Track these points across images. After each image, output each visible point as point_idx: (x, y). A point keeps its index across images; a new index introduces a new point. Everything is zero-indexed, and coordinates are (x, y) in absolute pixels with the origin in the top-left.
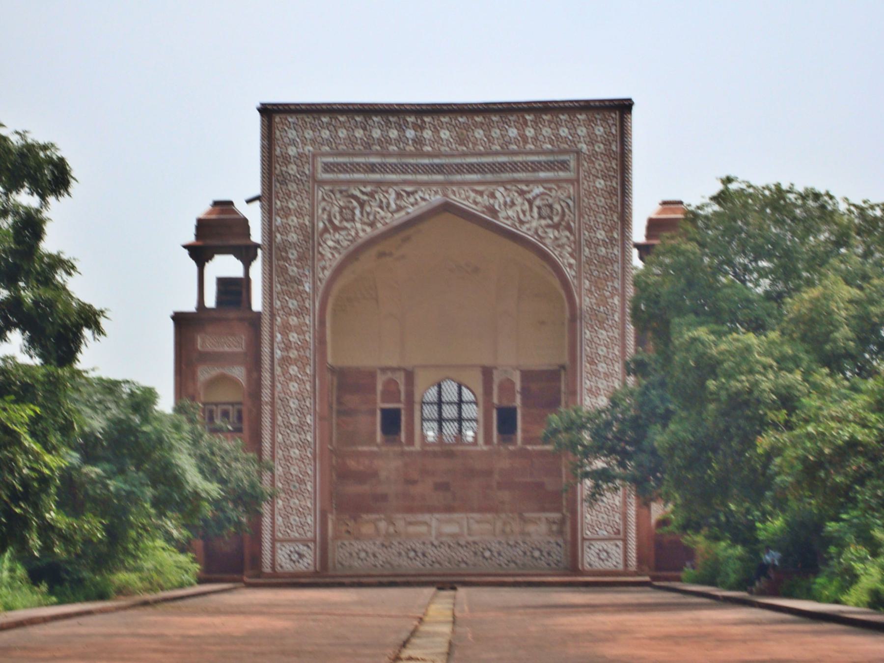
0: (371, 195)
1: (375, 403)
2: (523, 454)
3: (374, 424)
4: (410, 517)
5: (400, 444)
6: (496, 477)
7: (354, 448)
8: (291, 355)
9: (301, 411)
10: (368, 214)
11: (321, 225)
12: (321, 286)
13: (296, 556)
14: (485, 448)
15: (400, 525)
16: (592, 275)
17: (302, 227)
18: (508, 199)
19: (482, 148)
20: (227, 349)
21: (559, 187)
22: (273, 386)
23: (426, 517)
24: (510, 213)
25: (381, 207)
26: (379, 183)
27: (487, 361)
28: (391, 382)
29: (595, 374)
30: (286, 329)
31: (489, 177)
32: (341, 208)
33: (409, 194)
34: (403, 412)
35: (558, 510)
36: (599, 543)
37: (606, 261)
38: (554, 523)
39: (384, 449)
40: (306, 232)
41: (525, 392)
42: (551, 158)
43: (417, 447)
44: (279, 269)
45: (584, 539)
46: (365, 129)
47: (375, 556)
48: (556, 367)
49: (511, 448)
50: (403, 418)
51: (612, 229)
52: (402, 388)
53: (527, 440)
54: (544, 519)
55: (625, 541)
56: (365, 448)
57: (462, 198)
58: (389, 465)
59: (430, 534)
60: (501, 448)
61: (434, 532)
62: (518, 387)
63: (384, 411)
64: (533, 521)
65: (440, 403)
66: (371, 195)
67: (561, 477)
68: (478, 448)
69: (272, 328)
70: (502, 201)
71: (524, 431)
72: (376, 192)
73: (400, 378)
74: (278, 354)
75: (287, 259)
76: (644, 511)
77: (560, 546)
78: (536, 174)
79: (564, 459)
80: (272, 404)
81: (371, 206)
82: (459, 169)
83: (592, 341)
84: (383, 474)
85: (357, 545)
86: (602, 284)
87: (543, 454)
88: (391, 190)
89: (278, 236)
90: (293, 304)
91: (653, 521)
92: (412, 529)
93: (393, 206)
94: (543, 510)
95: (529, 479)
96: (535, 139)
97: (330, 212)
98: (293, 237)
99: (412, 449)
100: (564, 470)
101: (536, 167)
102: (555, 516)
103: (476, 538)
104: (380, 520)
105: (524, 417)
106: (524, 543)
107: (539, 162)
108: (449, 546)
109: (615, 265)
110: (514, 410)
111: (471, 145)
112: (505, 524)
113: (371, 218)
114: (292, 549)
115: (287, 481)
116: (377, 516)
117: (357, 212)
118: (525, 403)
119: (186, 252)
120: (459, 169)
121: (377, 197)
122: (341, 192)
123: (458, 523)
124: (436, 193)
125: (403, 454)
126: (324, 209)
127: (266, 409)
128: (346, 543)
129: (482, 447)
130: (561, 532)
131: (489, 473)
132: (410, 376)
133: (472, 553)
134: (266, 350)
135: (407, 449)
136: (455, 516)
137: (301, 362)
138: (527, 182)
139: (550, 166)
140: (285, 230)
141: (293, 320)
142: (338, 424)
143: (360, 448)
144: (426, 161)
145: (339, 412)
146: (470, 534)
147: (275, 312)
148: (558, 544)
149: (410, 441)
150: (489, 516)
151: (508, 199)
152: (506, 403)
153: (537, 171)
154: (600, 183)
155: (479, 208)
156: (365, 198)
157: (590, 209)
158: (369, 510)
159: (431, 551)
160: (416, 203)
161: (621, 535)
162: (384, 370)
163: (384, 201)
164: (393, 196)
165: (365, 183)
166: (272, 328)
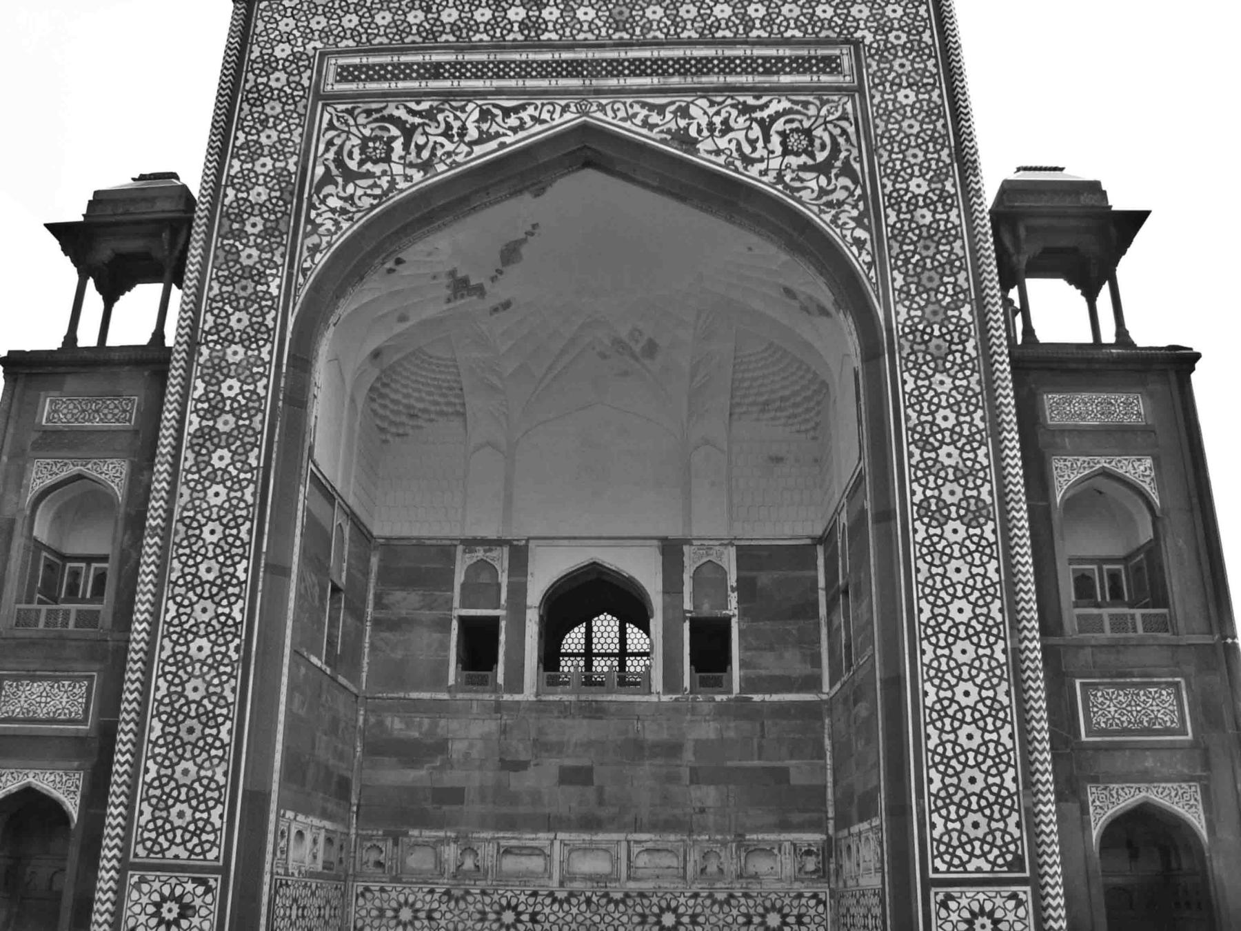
0: (430, 115)
1: (451, 609)
2: (741, 709)
3: (447, 648)
4: (509, 839)
5: (496, 689)
6: (688, 756)
7: (402, 695)
8: (220, 426)
9: (226, 552)
10: (420, 148)
11: (320, 171)
12: (305, 285)
13: (176, 908)
14: (665, 698)
15: (487, 853)
16: (907, 261)
17: (280, 175)
18: (717, 120)
19: (658, 34)
20: (97, 424)
21: (823, 103)
22: (172, 493)
23: (543, 838)
24: (722, 143)
25: (447, 134)
26: (447, 95)
27: (674, 532)
28: (483, 565)
29: (932, 469)
30: (218, 370)
31: (675, 81)
32: (365, 140)
33: (507, 112)
34: (503, 624)
35: (818, 826)
36: (970, 892)
37: (935, 236)
38: (809, 853)
39: (460, 696)
40: (288, 183)
41: (746, 588)
42: (804, 52)
43: (528, 694)
44: (221, 253)
45: (928, 884)
46: (428, 10)
47: (430, 918)
48: (808, 542)
49: (718, 698)
50: (502, 637)
51: (940, 176)
52: (504, 579)
53: (750, 684)
54: (787, 844)
55: (1037, 883)
56: (426, 695)
57: (616, 117)
58: (471, 734)
59: (550, 877)
60: (700, 698)
61: (556, 876)
62: (732, 580)
63: (463, 620)
64: (769, 853)
65: (588, 654)
66: (430, 115)
67: (823, 757)
68: (654, 699)
69: (188, 370)
70: (704, 122)
71: (743, 665)
72: (443, 111)
73: (501, 560)
74: (193, 423)
75: (240, 235)
76: (1074, 807)
77: (819, 902)
78: (775, 78)
79: (827, 721)
80: (166, 532)
81: (425, 133)
82: (615, 67)
83: (921, 398)
84: (457, 748)
85: (396, 894)
86: (930, 279)
87: (782, 710)
88: (470, 106)
89: (231, 192)
90: (239, 320)
91: (1095, 833)
92: (510, 864)
93: (473, 134)
94: (785, 826)
95: (756, 763)
96: (768, 21)
97: (341, 147)
98: (259, 194)
99: (517, 697)
100: (827, 742)
101: (772, 66)
102: (813, 838)
103: (647, 886)
104: (444, 841)
105: (740, 631)
106: (746, 895)
107: (781, 59)
108: (588, 901)
109: (958, 244)
110: (727, 621)
111: (638, 30)
112: (705, 856)
113: (425, 154)
114: (166, 890)
115: (174, 718)
116: (441, 834)
117: (398, 145)
118: (743, 614)
119: (54, 244)
120: (615, 67)
121: (440, 117)
122: (368, 113)
123: (606, 850)
124: (565, 109)
125: (499, 707)
126: (330, 143)
127: (151, 544)
128: (375, 887)
129: (658, 694)
130: (822, 873)
131: (673, 749)
132: (519, 557)
133: (636, 919)
134: (169, 415)
135: (507, 697)
136: (601, 837)
137: (238, 440)
138: (757, 91)
139: (799, 65)
140: (246, 181)
141: (236, 353)
142: (373, 647)
143: (414, 695)
144: (548, 56)
145: (377, 623)
146: (629, 878)
147: (200, 336)
148: (819, 902)
149: (515, 683)
150: (672, 837)
151: (717, 120)
152: (706, 610)
153: (777, 73)
154: (906, 96)
155: (654, 134)
156: (417, 120)
157: (892, 140)
158: (424, 821)
159: (547, 910)
160: (522, 127)
161: (1022, 870)
162: (471, 544)
163: (456, 125)
164: (476, 115)
165: (418, 96)
166: (188, 370)
